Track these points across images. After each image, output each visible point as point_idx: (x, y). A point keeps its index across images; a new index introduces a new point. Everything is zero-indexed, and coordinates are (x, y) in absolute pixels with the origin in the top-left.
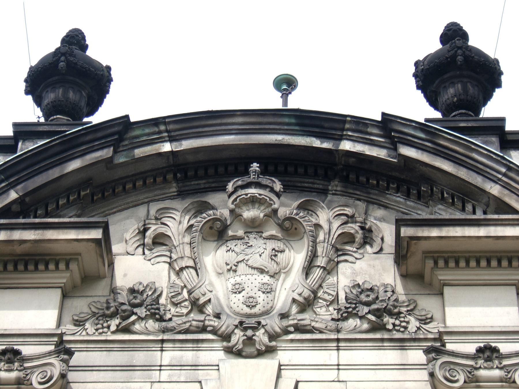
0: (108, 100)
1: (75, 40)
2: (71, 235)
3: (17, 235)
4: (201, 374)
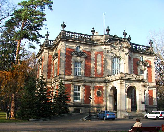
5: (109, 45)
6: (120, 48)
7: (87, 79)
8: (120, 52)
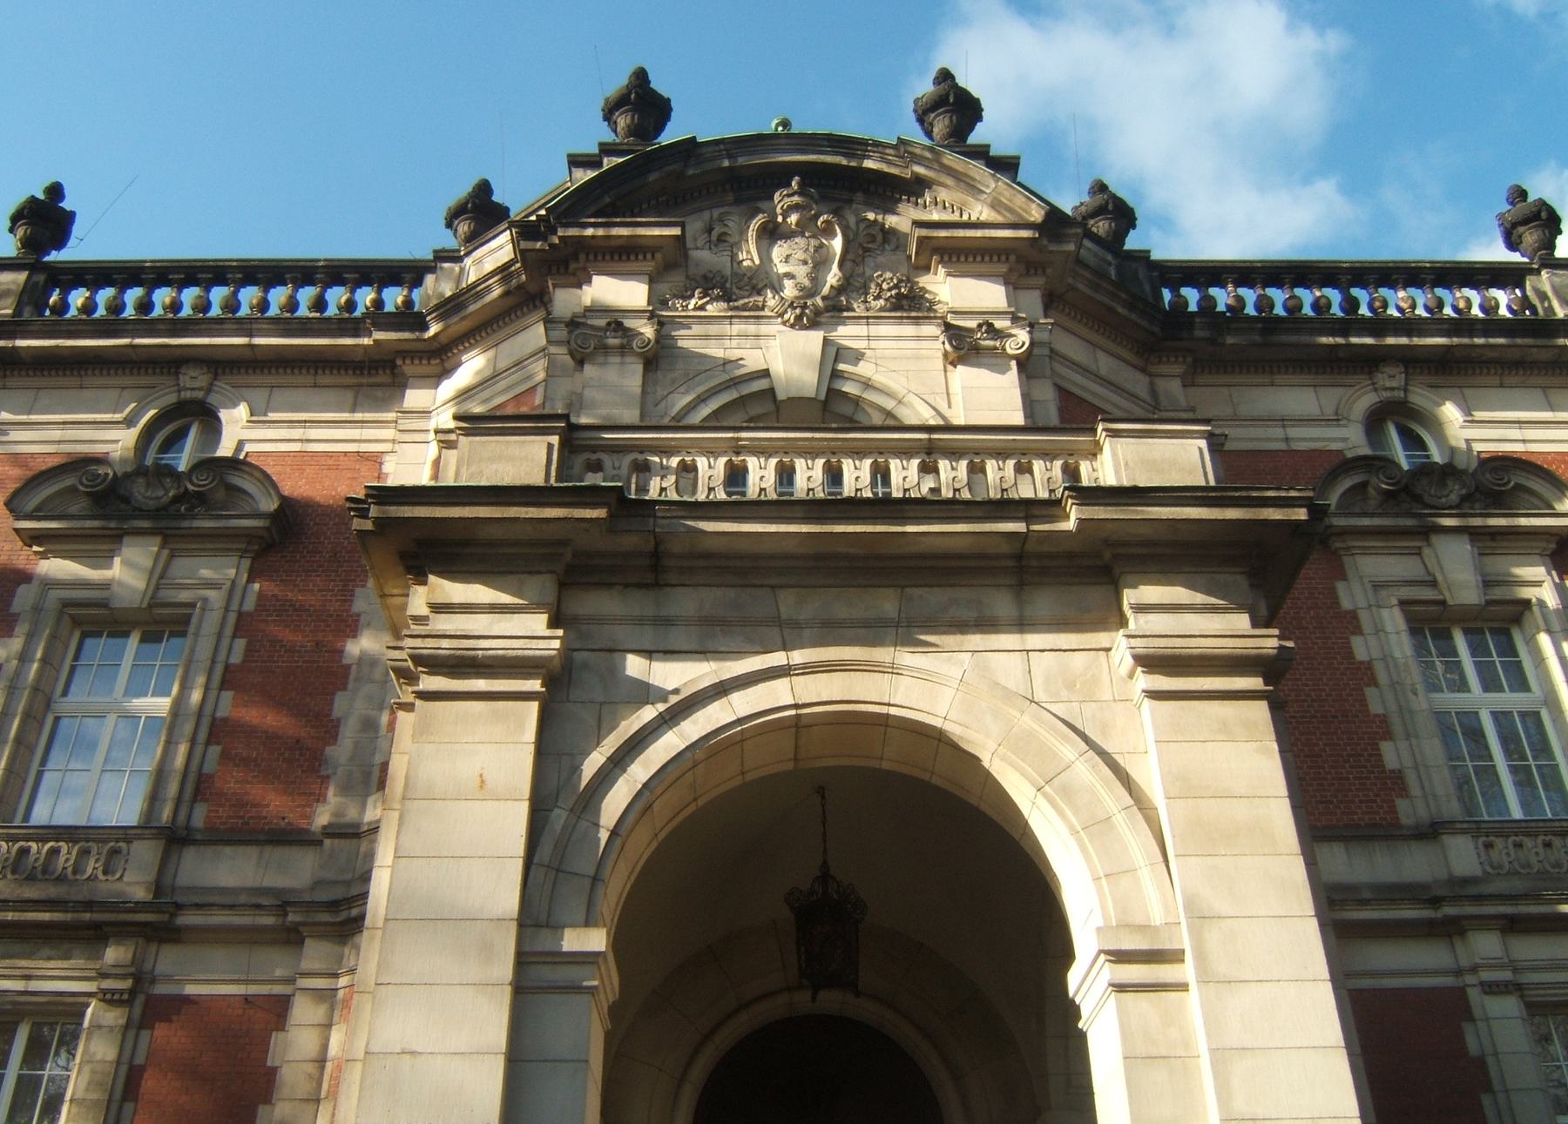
0: (670, 126)
1: (641, 76)
2: (657, 232)
3: (616, 231)
4: (762, 342)
5: (619, 257)
6: (833, 277)
7: (231, 870)
8: (848, 334)
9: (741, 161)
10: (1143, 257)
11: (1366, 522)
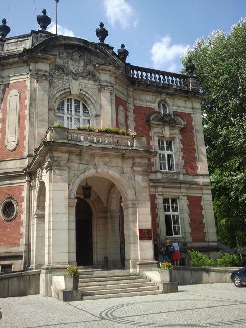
9: (67, 42)
10: (129, 64)
11: (155, 123)
